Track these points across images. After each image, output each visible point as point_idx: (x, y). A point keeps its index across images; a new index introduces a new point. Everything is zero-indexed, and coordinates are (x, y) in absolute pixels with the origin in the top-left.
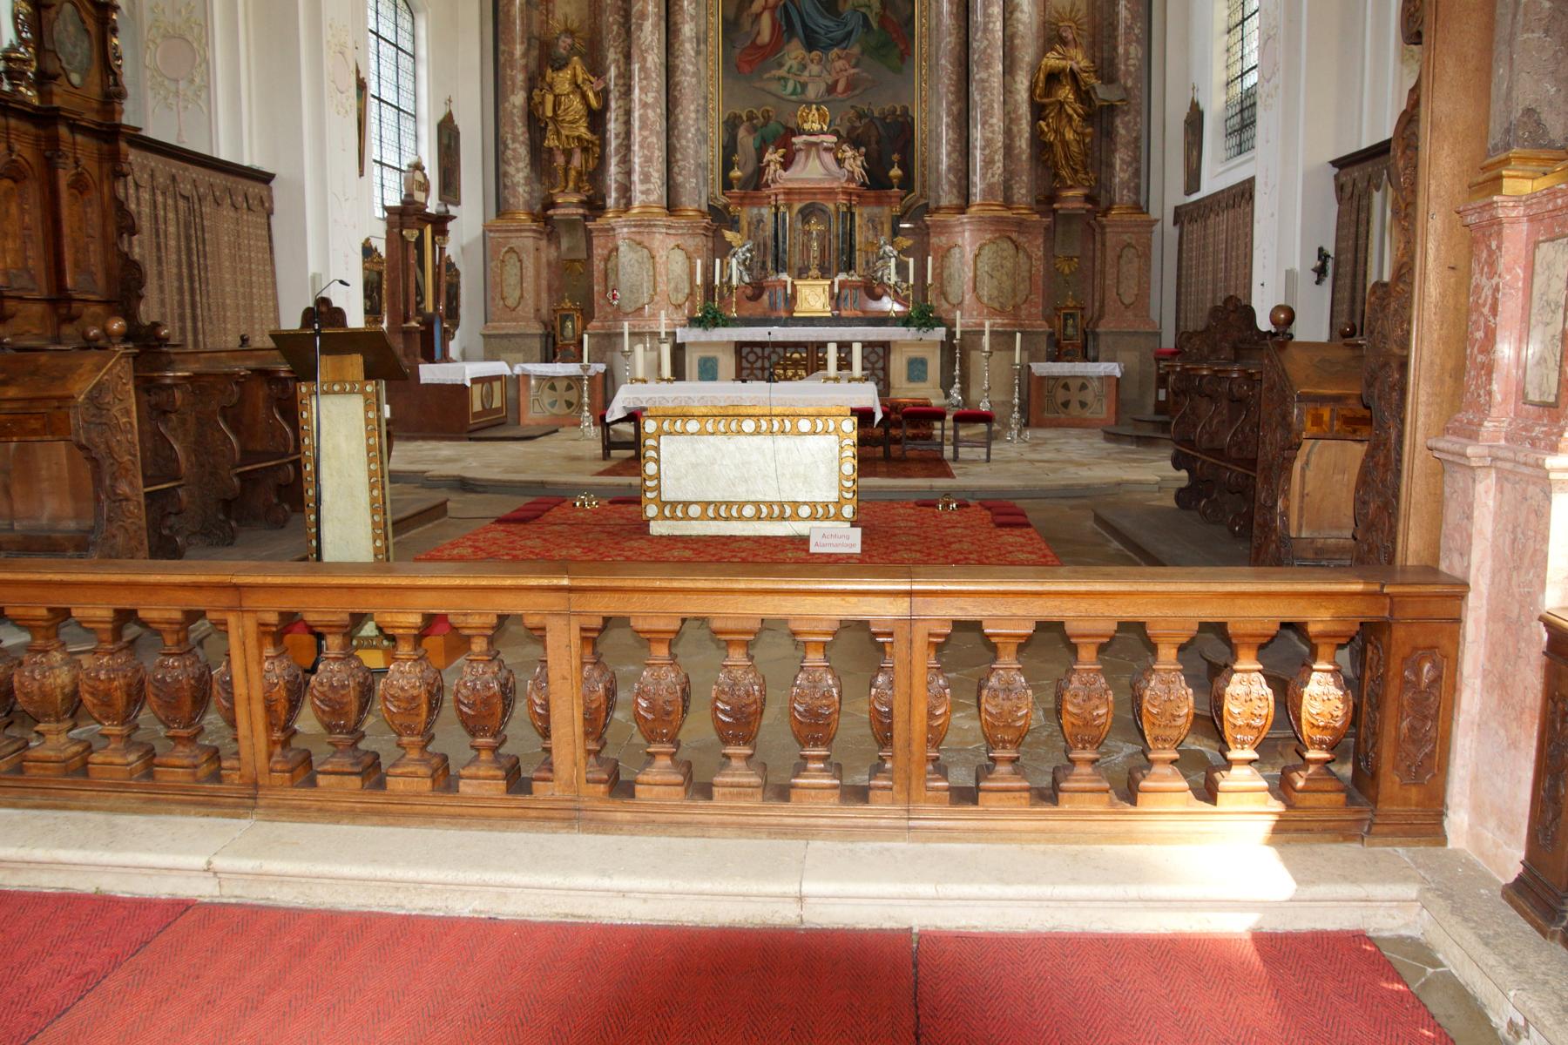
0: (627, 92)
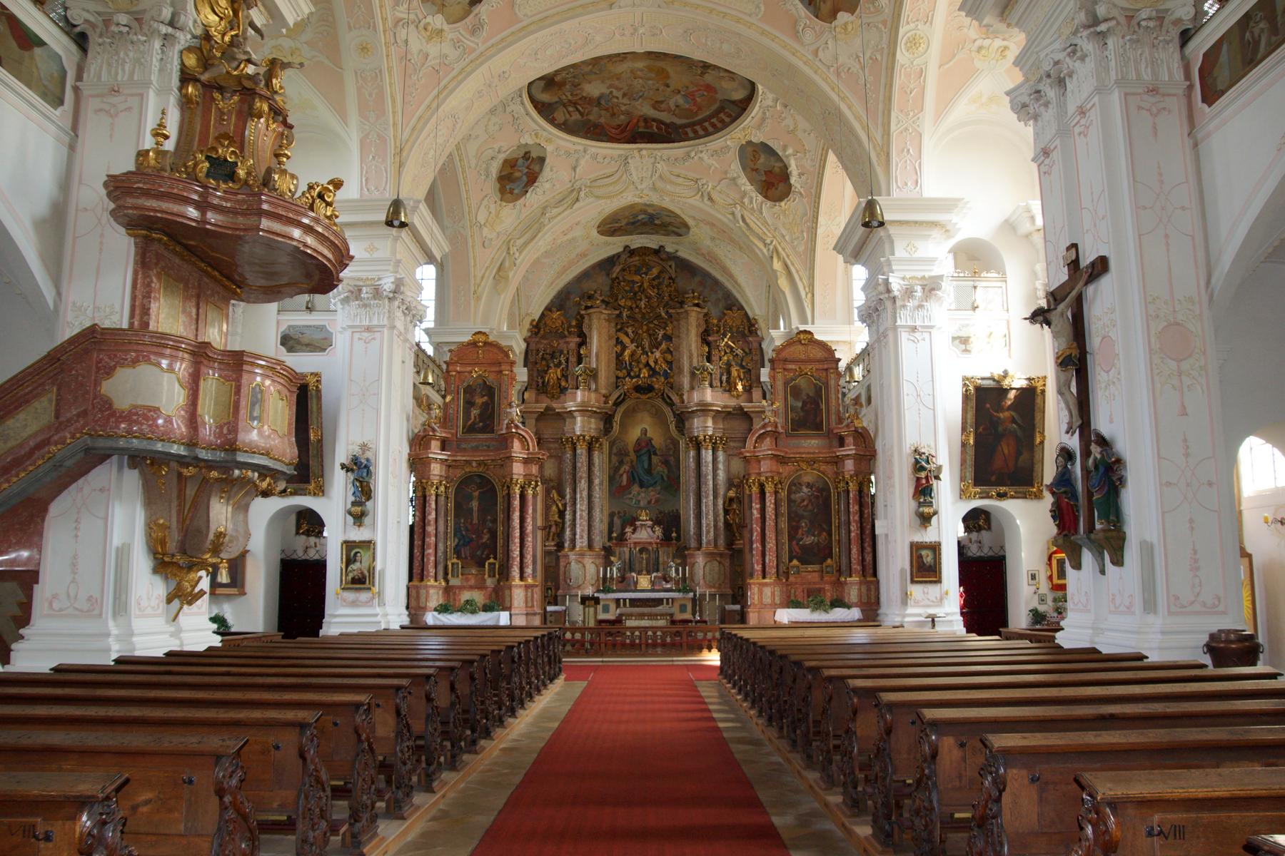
0: (574, 504)
